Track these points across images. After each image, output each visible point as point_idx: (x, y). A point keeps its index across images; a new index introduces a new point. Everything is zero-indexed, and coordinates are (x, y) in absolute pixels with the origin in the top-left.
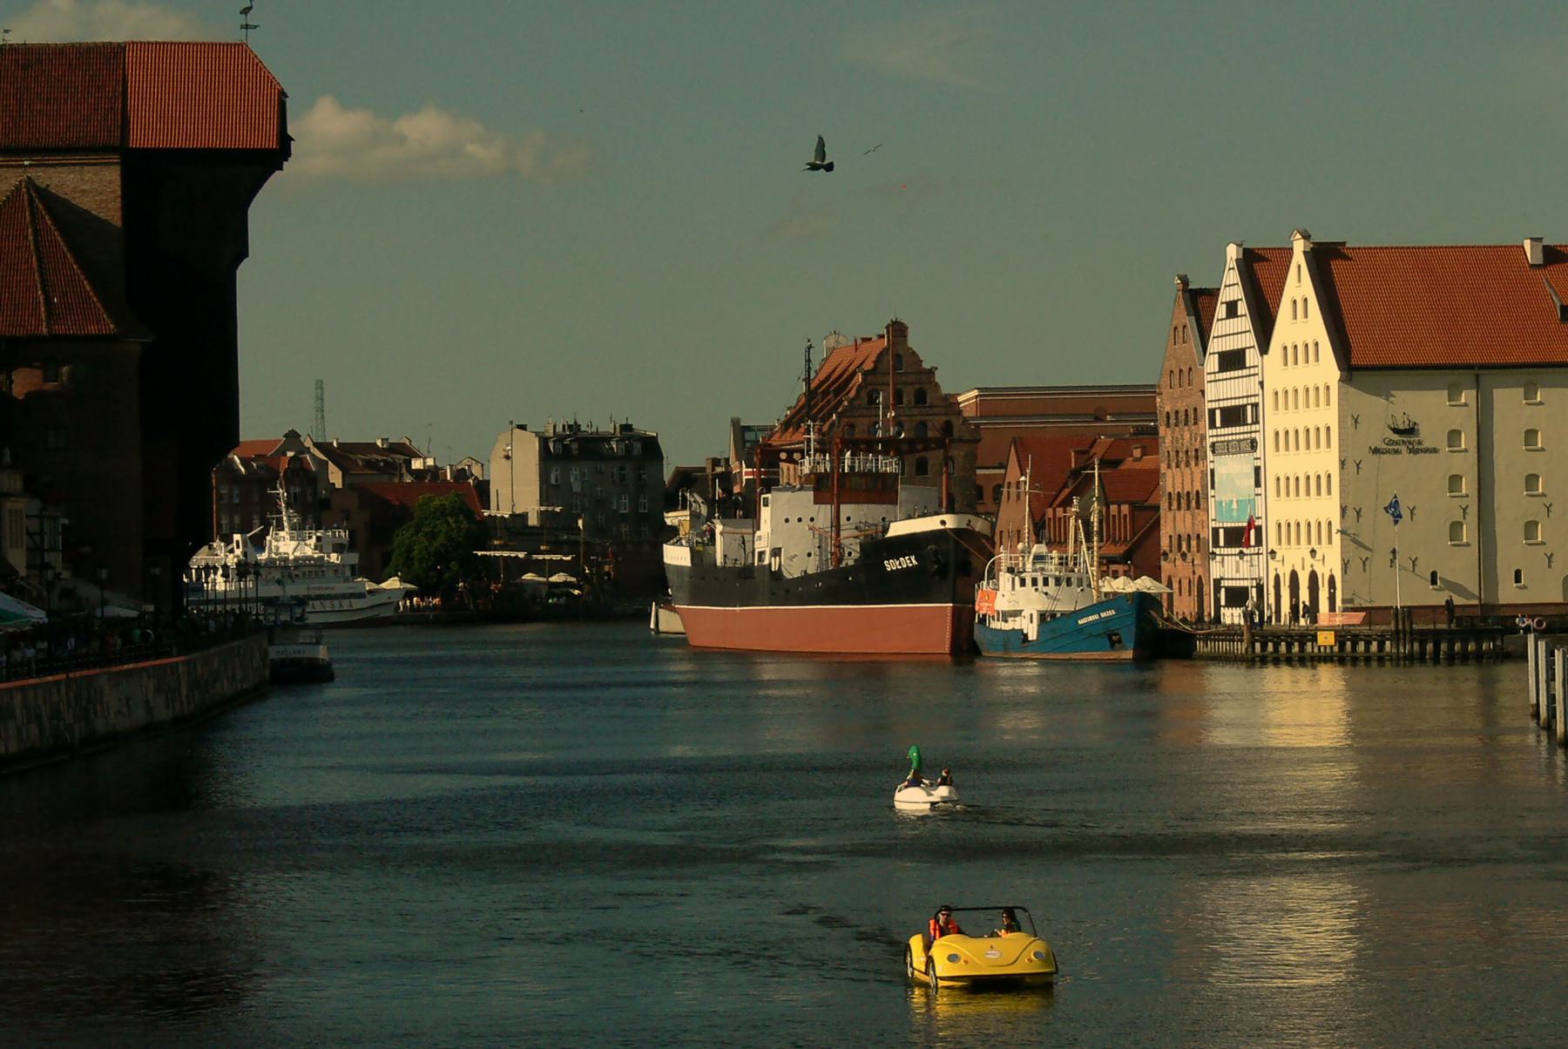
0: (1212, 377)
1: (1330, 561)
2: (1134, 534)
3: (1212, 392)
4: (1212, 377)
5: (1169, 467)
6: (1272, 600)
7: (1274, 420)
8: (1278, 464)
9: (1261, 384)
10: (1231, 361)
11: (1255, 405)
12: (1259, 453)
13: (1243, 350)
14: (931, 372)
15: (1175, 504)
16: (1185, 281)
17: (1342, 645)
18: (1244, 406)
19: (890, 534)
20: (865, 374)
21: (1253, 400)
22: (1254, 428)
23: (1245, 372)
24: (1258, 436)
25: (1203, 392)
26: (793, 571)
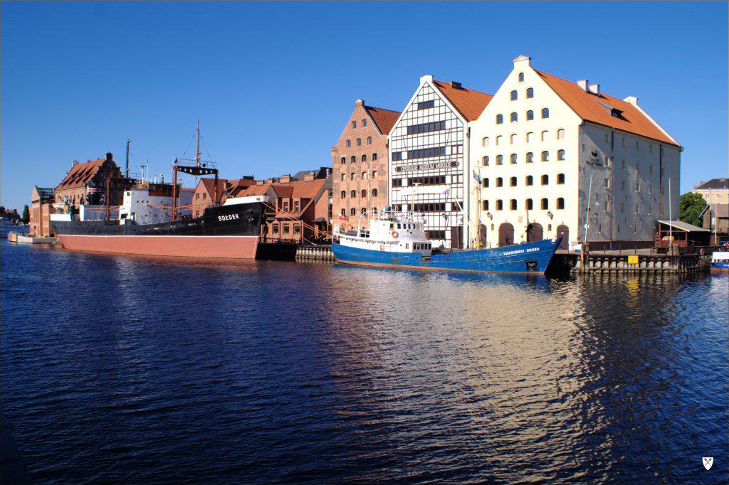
0: (400, 138)
1: (569, 217)
2: (302, 209)
4: (400, 138)
5: (342, 180)
7: (477, 153)
10: (440, 126)
11: (457, 146)
12: (460, 167)
14: (119, 168)
15: (348, 195)
16: (363, 102)
17: (640, 262)
18: (444, 147)
19: (225, 205)
20: (100, 167)
21: (455, 143)
22: (453, 156)
23: (442, 132)
25: (387, 146)
26: (140, 222)
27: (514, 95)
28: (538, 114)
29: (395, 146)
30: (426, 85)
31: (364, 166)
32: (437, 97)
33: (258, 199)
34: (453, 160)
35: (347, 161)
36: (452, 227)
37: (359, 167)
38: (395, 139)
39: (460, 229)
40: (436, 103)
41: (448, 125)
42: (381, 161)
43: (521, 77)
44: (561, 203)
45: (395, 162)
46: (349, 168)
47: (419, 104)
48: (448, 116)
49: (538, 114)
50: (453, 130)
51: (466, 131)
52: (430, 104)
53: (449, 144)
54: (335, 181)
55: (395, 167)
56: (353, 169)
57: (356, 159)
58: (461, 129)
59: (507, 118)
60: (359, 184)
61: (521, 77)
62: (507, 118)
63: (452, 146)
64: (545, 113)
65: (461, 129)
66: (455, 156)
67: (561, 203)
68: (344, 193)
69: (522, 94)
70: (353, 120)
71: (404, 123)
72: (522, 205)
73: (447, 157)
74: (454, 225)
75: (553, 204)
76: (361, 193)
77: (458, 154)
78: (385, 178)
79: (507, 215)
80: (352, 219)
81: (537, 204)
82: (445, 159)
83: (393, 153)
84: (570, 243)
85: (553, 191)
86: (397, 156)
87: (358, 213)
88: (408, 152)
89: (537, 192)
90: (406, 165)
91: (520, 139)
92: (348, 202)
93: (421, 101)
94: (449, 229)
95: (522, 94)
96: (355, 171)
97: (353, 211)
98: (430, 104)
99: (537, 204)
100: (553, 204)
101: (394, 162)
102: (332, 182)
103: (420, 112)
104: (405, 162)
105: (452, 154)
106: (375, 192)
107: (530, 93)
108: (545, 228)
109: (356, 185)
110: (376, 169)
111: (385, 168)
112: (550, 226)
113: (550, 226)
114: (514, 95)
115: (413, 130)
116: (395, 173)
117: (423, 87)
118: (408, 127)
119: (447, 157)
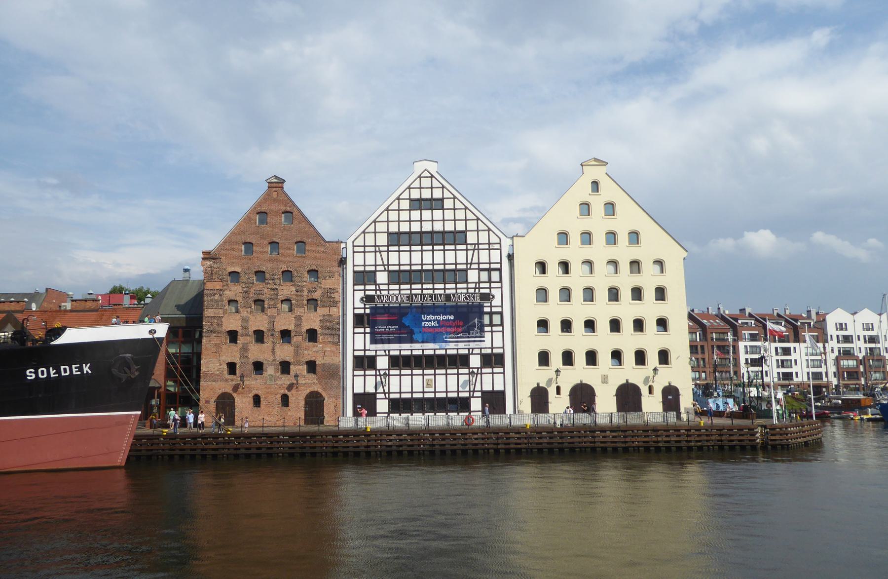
0: (373, 249)
1: (681, 375)
3: (356, 261)
4: (373, 249)
6: (526, 405)
7: (528, 280)
8: (529, 312)
9: (511, 257)
11: (489, 270)
12: (496, 302)
13: (455, 233)
18: (466, 271)
21: (487, 266)
22: (482, 285)
24: (496, 292)
25: (343, 262)
27: (586, 208)
28: (623, 238)
29: (356, 261)
30: (426, 174)
31: (287, 290)
32: (447, 194)
33: (152, 332)
34: (482, 291)
35: (243, 278)
36: (483, 392)
37: (276, 290)
38: (362, 249)
39: (502, 393)
40: (448, 204)
41: (471, 238)
42: (327, 283)
43: (595, 185)
44: (664, 357)
45: (362, 287)
46: (246, 293)
47: (411, 200)
48: (472, 225)
49: (623, 238)
50: (481, 247)
51: (505, 251)
52: (435, 204)
53: (476, 266)
54: (208, 313)
55: (359, 295)
56: (260, 292)
57: (267, 275)
58: (498, 246)
59: (575, 238)
60: (272, 320)
61: (595, 185)
62: (575, 238)
63: (480, 270)
64: (635, 237)
65: (498, 246)
66: (488, 285)
67: (664, 357)
68: (233, 336)
69: (598, 209)
70: (259, 209)
71: (382, 227)
72: (604, 358)
73: (470, 286)
74: (487, 387)
75: (652, 359)
76: (278, 335)
77: (490, 281)
78: (335, 309)
79: (579, 373)
80: (255, 383)
81: (629, 358)
82: (467, 289)
83: (354, 272)
84: (682, 410)
85: (652, 341)
86: (364, 277)
87: (270, 371)
88: (389, 272)
89: (628, 341)
90: (383, 292)
91: (601, 266)
92: (245, 350)
93: (415, 194)
94: (479, 394)
95: (598, 209)
96: (261, 297)
97: (258, 367)
98: (435, 204)
99: (629, 358)
100: (652, 359)
101: (357, 287)
102: (202, 314)
103: (416, 214)
104: (386, 287)
105: (479, 282)
106: (312, 335)
107: (610, 208)
108: (644, 390)
109: (266, 322)
110: (317, 295)
111: (336, 295)
112: (651, 388)
113: (651, 388)
114: (586, 208)
115: (397, 239)
116: (358, 304)
117: (420, 177)
118: (390, 234)
119: (473, 285)
